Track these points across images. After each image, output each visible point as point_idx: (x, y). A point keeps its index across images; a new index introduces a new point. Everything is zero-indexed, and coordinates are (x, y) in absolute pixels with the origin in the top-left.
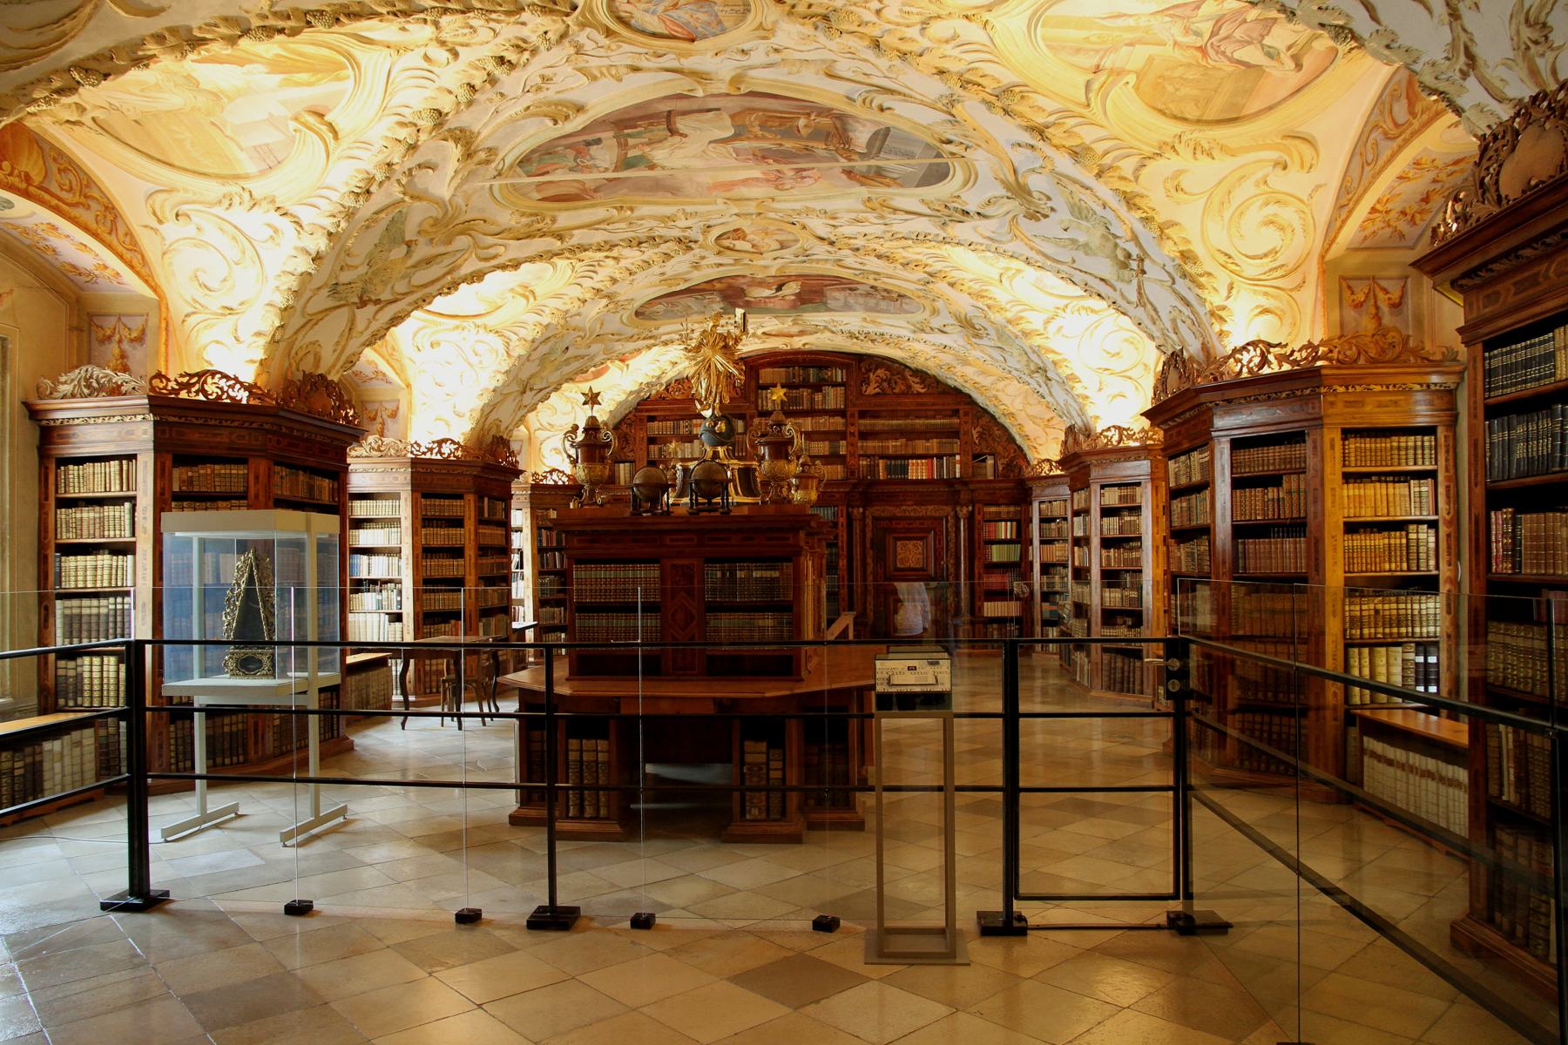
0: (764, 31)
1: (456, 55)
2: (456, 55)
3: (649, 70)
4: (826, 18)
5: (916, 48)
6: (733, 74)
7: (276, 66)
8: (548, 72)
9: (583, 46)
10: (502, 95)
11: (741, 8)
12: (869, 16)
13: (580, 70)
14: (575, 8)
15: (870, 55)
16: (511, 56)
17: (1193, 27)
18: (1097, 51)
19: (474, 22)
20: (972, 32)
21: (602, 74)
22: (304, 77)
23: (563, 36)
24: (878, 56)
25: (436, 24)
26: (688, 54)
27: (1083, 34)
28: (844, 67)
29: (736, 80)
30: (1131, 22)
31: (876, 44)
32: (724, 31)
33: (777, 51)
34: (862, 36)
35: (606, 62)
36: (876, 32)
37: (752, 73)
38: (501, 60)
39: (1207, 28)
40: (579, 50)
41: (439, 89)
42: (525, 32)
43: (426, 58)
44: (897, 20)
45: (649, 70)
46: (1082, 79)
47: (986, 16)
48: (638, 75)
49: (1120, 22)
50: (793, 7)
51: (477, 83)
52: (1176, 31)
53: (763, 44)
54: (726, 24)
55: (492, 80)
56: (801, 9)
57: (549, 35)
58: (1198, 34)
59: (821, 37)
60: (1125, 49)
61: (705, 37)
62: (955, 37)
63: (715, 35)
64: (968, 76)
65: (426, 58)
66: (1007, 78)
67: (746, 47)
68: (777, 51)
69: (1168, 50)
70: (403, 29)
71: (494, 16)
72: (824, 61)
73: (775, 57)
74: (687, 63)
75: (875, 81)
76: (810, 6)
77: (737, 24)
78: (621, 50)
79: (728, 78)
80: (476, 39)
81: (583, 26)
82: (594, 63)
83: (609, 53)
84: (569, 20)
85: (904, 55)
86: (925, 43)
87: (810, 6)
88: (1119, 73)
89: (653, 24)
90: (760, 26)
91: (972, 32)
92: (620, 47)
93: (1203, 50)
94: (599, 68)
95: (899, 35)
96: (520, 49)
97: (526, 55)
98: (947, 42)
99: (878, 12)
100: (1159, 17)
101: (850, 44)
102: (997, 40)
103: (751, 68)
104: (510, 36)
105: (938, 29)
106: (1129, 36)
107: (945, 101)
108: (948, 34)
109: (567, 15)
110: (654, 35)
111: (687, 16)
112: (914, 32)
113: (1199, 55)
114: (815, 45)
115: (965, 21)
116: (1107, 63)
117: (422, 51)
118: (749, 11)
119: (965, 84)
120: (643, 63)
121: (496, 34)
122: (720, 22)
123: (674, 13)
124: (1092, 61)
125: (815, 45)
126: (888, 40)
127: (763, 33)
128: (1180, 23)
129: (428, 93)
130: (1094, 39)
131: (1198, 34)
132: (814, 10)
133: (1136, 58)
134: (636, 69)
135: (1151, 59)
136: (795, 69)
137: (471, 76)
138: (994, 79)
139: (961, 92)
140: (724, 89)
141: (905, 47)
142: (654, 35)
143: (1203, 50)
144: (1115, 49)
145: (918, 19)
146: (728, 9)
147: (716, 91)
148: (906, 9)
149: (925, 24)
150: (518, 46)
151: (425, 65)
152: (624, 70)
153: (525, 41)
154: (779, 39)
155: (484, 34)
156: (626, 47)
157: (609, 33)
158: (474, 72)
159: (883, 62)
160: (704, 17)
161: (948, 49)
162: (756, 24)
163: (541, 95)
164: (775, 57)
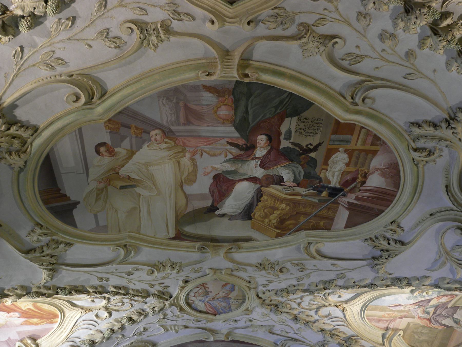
0: (248, 311)
1: (110, 314)
2: (110, 314)
3: (192, 328)
4: (277, 306)
5: (312, 319)
6: (228, 331)
7: (26, 314)
8: (147, 326)
9: (167, 315)
10: (123, 335)
11: (241, 301)
12: (295, 305)
13: (162, 326)
14: (171, 297)
15: (292, 324)
16: (135, 317)
17: (426, 310)
18: (387, 321)
19: (125, 301)
20: (337, 313)
21: (171, 328)
22: (35, 320)
23: (162, 309)
24: (296, 323)
25: (109, 299)
26: (211, 321)
27: (382, 313)
28: (277, 329)
29: (229, 334)
30: (402, 308)
31: (296, 318)
32: (230, 311)
33: (250, 321)
34: (290, 314)
35: (175, 323)
36: (296, 312)
37: (236, 331)
38: (130, 319)
39: (432, 310)
40: (165, 317)
41: (98, 331)
42: (145, 307)
43: (97, 316)
44: (307, 307)
45: (192, 328)
46: (380, 333)
47: (345, 305)
48: (187, 330)
49: (398, 308)
50: (264, 301)
51: (116, 328)
52: (419, 311)
53: (245, 317)
54: (232, 308)
55: (123, 328)
56: (267, 302)
57: (156, 308)
58: (428, 313)
59: (272, 316)
60: (399, 320)
61: (221, 313)
62: (330, 314)
63: (226, 313)
64: (333, 332)
65: (97, 316)
66: (349, 332)
67: (237, 319)
68: (250, 321)
69: (416, 320)
70: (93, 301)
71: (136, 298)
72: (269, 326)
73: (249, 323)
74: (209, 325)
75: (290, 335)
76: (271, 301)
77: (237, 309)
78: (183, 318)
79: (226, 333)
80: (123, 308)
81: (171, 305)
82: (169, 323)
83: (178, 319)
84: (167, 303)
85: (307, 323)
86: (316, 317)
87: (271, 301)
88: (396, 330)
89: (201, 306)
90: (247, 309)
91: (337, 313)
92: (183, 316)
93: (429, 320)
94: (171, 326)
95: (306, 314)
96: (140, 314)
97: (142, 317)
98: (326, 317)
99: (299, 304)
100: (413, 306)
101: (284, 318)
102: (347, 316)
103: (237, 328)
104: (138, 308)
105: (323, 311)
106: (400, 314)
107: (320, 344)
108: (327, 313)
109: (167, 300)
110: (200, 312)
111: (217, 304)
112: (312, 313)
113: (428, 322)
114: (268, 318)
115: (336, 308)
116: (391, 326)
117: (95, 312)
118: (244, 302)
119: (332, 335)
120: (191, 324)
121: (132, 306)
122: (230, 307)
123: (212, 302)
124: (384, 325)
125: (268, 318)
126: (302, 316)
127: (247, 312)
128: (422, 309)
129: (91, 332)
130: (386, 315)
131: (428, 313)
132: (272, 302)
133: (402, 324)
134: (186, 327)
135: (409, 324)
136: (256, 329)
137: (114, 325)
138: (344, 333)
139: (330, 339)
140: (222, 338)
141: (308, 319)
142: (200, 312)
143: (429, 320)
144: (394, 319)
145: (315, 307)
146: (235, 301)
147: (218, 339)
148: (312, 302)
149: (319, 308)
150: (140, 313)
151: (95, 318)
152: (181, 327)
153: (143, 311)
154: (254, 315)
155: (128, 306)
156: (186, 316)
157: (181, 309)
158: (116, 324)
159: (296, 326)
160: (223, 304)
161: (325, 320)
162: (245, 308)
163: (140, 337)
164: (249, 323)
